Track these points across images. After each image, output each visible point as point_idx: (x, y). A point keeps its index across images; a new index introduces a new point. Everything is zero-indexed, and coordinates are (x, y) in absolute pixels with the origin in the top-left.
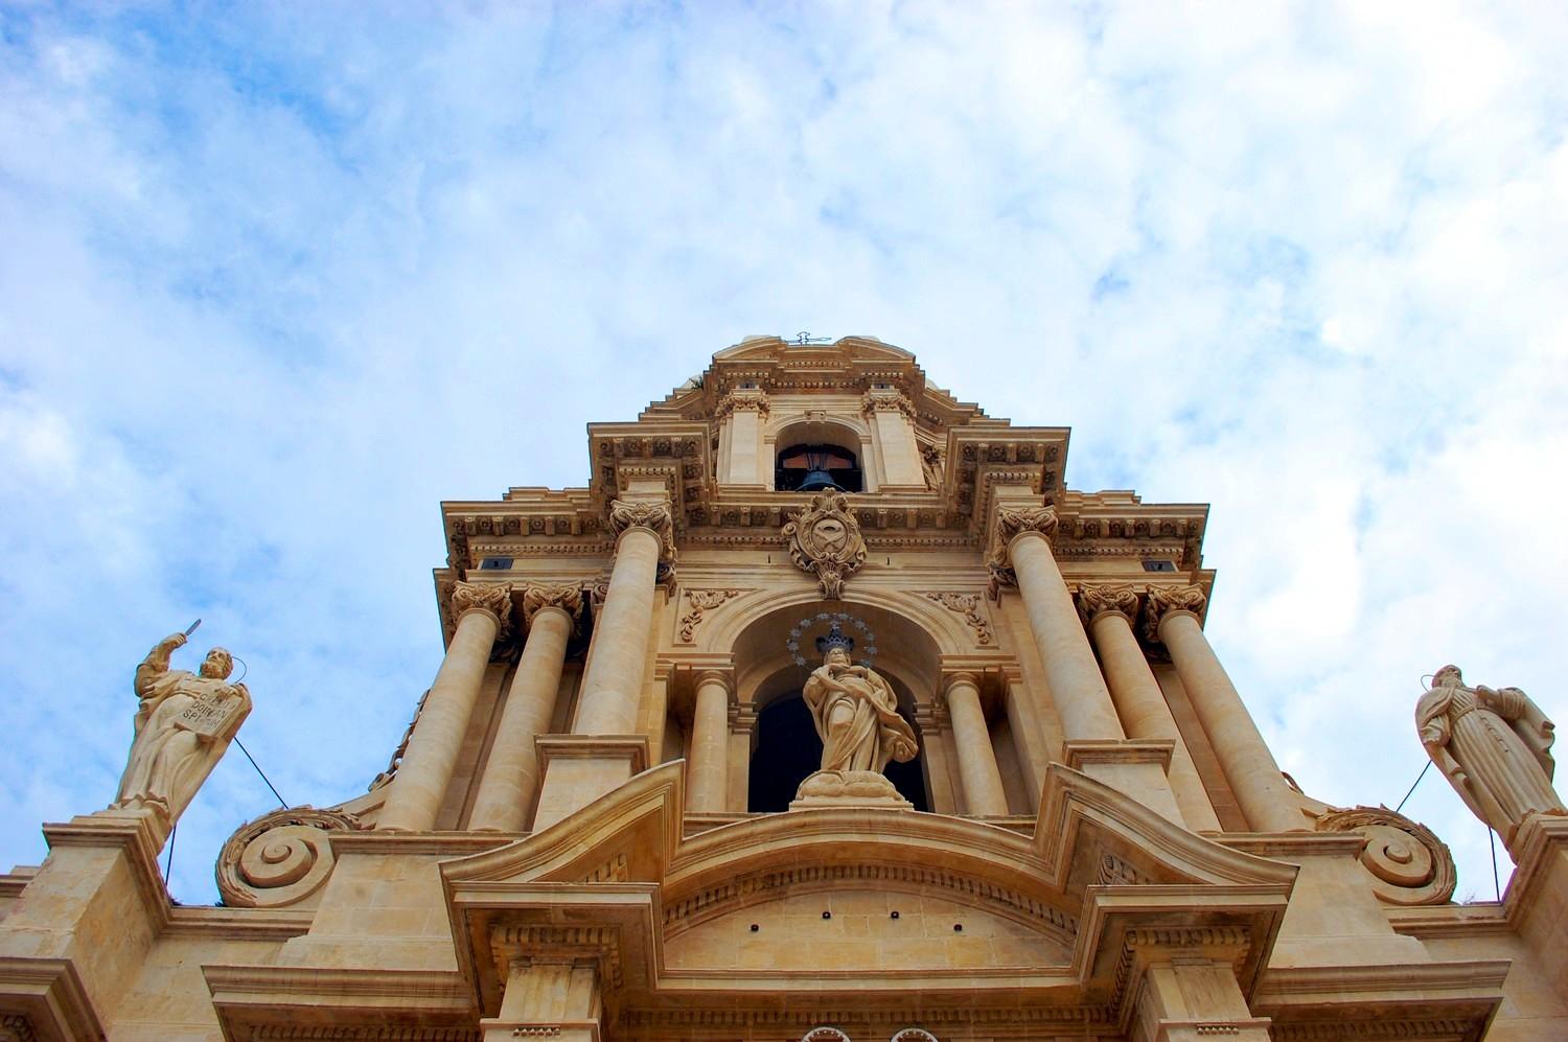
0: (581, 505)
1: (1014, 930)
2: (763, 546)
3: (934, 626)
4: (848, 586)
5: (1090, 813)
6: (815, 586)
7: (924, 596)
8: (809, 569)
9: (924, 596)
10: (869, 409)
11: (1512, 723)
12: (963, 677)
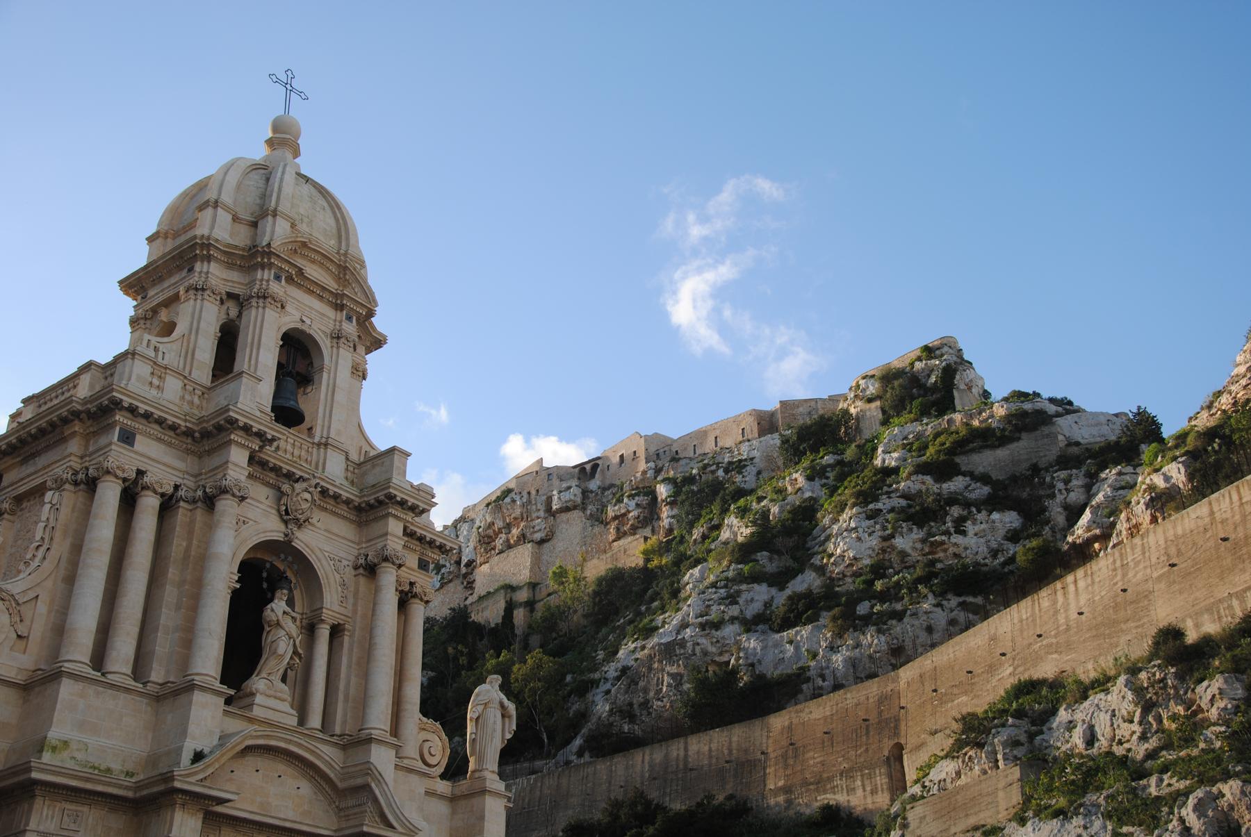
0: (190, 422)
1: (315, 793)
2: (268, 484)
3: (326, 581)
4: (298, 534)
5: (373, 785)
6: (282, 527)
7: (327, 554)
8: (287, 516)
9: (327, 554)
10: (337, 337)
11: (503, 716)
12: (328, 624)
